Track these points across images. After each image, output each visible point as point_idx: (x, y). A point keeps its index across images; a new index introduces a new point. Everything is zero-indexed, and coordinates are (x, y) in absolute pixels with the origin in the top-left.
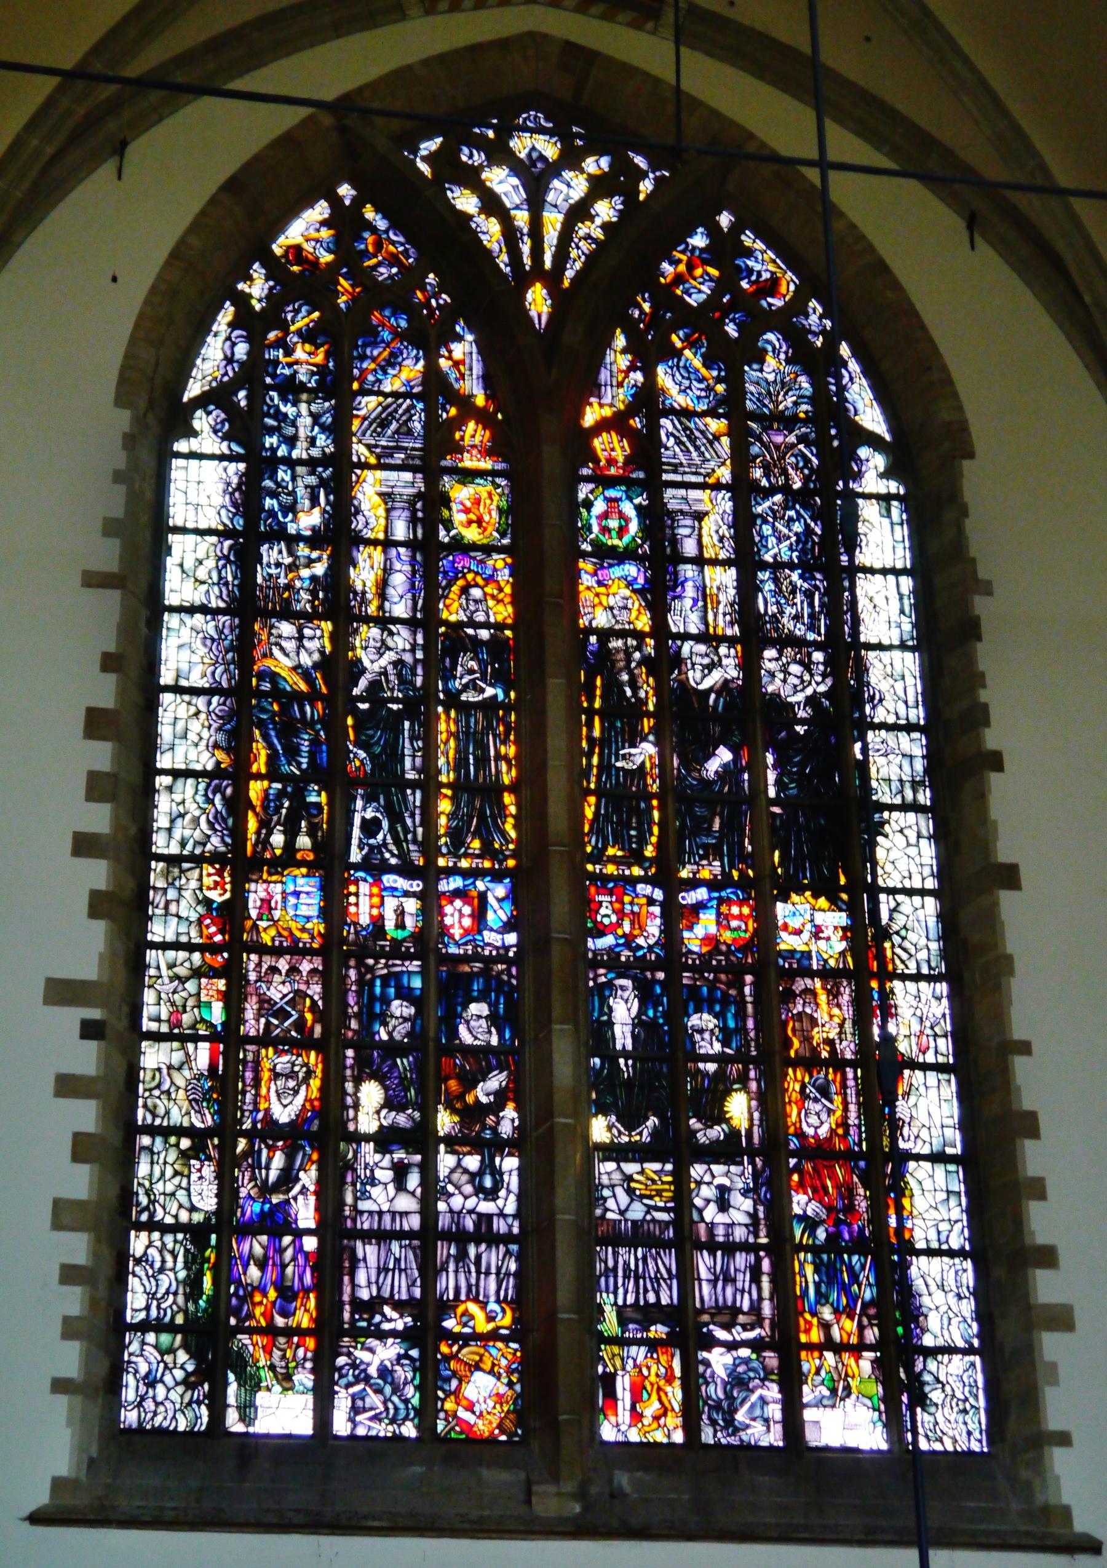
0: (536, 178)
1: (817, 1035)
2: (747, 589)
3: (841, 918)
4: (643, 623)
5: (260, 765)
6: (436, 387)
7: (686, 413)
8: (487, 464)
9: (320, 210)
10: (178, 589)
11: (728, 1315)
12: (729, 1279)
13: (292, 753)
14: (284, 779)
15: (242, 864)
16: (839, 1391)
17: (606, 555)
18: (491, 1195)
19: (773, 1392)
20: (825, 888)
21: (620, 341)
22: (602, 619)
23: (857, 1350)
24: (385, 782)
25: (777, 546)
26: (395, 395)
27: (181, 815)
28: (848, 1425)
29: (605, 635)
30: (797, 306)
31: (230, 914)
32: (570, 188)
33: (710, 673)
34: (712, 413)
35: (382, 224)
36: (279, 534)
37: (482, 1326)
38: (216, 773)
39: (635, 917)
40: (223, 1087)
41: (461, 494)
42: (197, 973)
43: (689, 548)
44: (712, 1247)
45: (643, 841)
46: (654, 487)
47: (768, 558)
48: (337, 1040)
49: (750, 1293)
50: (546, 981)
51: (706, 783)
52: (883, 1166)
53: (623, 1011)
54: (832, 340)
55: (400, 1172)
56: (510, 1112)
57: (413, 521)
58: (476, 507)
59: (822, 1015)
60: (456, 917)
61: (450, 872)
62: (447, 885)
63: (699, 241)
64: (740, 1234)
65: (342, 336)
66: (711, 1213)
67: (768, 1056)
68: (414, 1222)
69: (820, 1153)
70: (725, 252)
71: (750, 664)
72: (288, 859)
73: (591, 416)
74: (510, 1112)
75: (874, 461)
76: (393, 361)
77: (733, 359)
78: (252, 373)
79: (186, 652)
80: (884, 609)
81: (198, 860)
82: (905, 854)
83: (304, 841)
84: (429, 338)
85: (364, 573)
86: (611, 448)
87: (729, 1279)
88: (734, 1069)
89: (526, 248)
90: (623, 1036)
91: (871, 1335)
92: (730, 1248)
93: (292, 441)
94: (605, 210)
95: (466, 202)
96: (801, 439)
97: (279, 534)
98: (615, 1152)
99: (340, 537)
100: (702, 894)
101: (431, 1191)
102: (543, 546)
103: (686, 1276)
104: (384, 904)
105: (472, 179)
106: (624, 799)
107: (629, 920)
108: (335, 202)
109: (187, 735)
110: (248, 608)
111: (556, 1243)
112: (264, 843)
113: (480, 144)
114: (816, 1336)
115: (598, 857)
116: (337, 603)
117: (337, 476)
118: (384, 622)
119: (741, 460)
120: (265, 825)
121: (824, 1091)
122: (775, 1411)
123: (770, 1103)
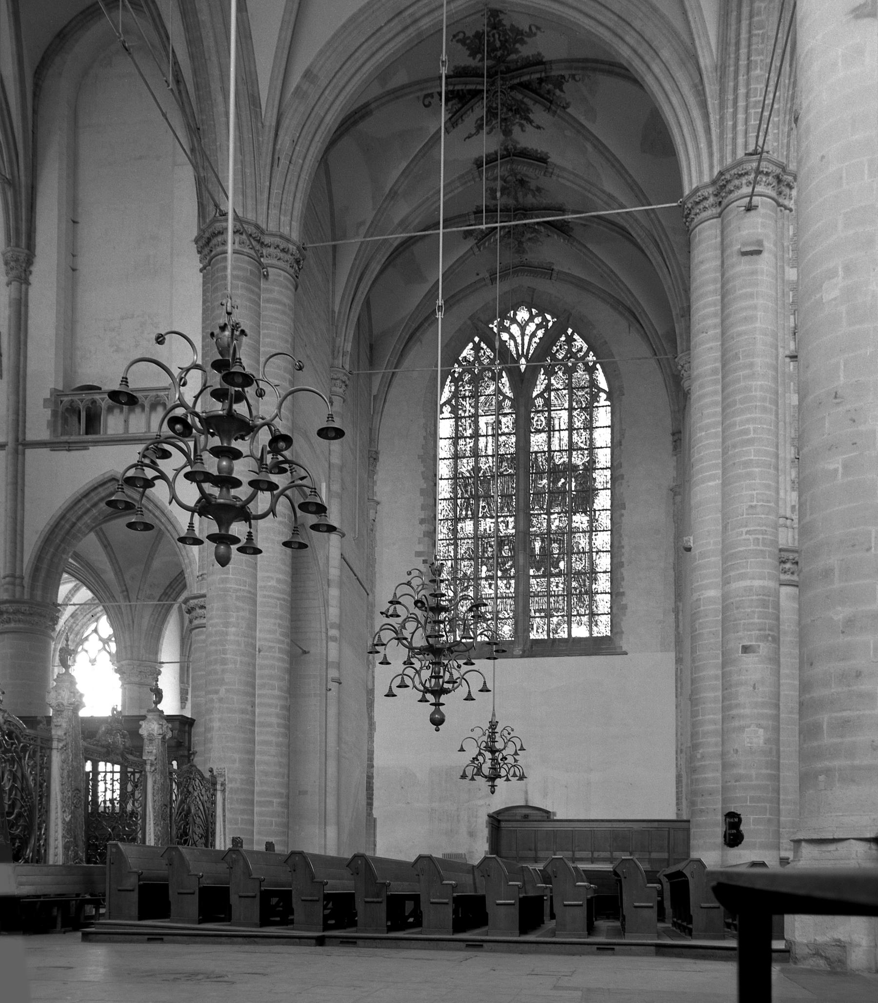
0: (523, 329)
1: (580, 547)
2: (570, 437)
3: (588, 518)
4: (546, 449)
5: (459, 496)
6: (498, 391)
7: (558, 389)
8: (510, 411)
9: (471, 345)
10: (442, 454)
11: (557, 610)
12: (558, 602)
13: (467, 491)
14: (465, 498)
15: (456, 520)
16: (580, 623)
17: (538, 431)
18: (509, 588)
19: (566, 626)
20: (585, 512)
21: (542, 372)
22: (536, 449)
23: (584, 615)
24: (487, 497)
25: (578, 424)
26: (488, 395)
27: (443, 508)
28: (580, 631)
29: (536, 453)
30: (587, 354)
31: (455, 531)
32: (531, 327)
33: (560, 459)
34: (564, 389)
35: (485, 347)
36: (463, 437)
37: (507, 616)
38: (451, 498)
39: (541, 523)
40: (455, 569)
41: (504, 420)
42: (448, 545)
43: (557, 428)
44: (554, 596)
45: (543, 504)
46: (549, 411)
47: (575, 426)
48: (476, 557)
49: (562, 604)
50: (524, 535)
51: (558, 488)
52: (592, 573)
53: (538, 545)
54: (595, 363)
55: (490, 585)
56: (513, 570)
57: (493, 429)
58: (507, 422)
59: (581, 542)
60: (502, 527)
61: (500, 517)
62: (500, 520)
63: (563, 338)
64: (560, 593)
65: (476, 380)
66: (555, 588)
67: (569, 552)
68: (493, 595)
69: (579, 573)
70: (570, 340)
71: (570, 457)
72: (466, 517)
73: (535, 394)
74: (513, 570)
75: (603, 396)
76: (488, 386)
77: (570, 371)
78: (455, 395)
79: (444, 469)
80: (603, 437)
81: (447, 520)
82: (603, 500)
83: (469, 513)
84: (496, 378)
85: (482, 441)
86: (540, 402)
87: (558, 602)
88: (561, 556)
89: (520, 348)
90: (537, 551)
91: (587, 612)
92: (558, 596)
93: (465, 411)
94: (540, 333)
95: (505, 336)
96: (586, 393)
97: (463, 437)
98: (535, 577)
99: (476, 435)
100: (556, 516)
101: (497, 587)
102: (523, 430)
103: (549, 603)
104: (487, 525)
105: (507, 330)
106: (539, 494)
107: (540, 524)
108: (474, 342)
109: (444, 489)
110: (456, 457)
111: (523, 596)
112: (461, 514)
113: (509, 318)
114: (575, 613)
115: (533, 509)
116: (475, 453)
117: (475, 417)
118: (487, 456)
119: (571, 401)
120: (461, 510)
121: (581, 559)
122: (566, 630)
123: (569, 563)
